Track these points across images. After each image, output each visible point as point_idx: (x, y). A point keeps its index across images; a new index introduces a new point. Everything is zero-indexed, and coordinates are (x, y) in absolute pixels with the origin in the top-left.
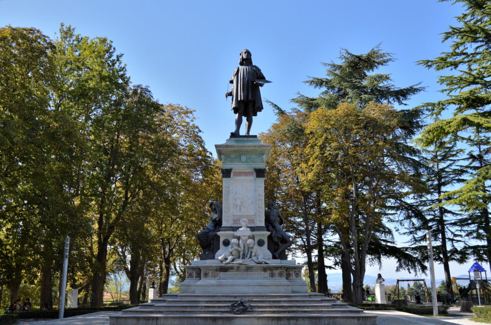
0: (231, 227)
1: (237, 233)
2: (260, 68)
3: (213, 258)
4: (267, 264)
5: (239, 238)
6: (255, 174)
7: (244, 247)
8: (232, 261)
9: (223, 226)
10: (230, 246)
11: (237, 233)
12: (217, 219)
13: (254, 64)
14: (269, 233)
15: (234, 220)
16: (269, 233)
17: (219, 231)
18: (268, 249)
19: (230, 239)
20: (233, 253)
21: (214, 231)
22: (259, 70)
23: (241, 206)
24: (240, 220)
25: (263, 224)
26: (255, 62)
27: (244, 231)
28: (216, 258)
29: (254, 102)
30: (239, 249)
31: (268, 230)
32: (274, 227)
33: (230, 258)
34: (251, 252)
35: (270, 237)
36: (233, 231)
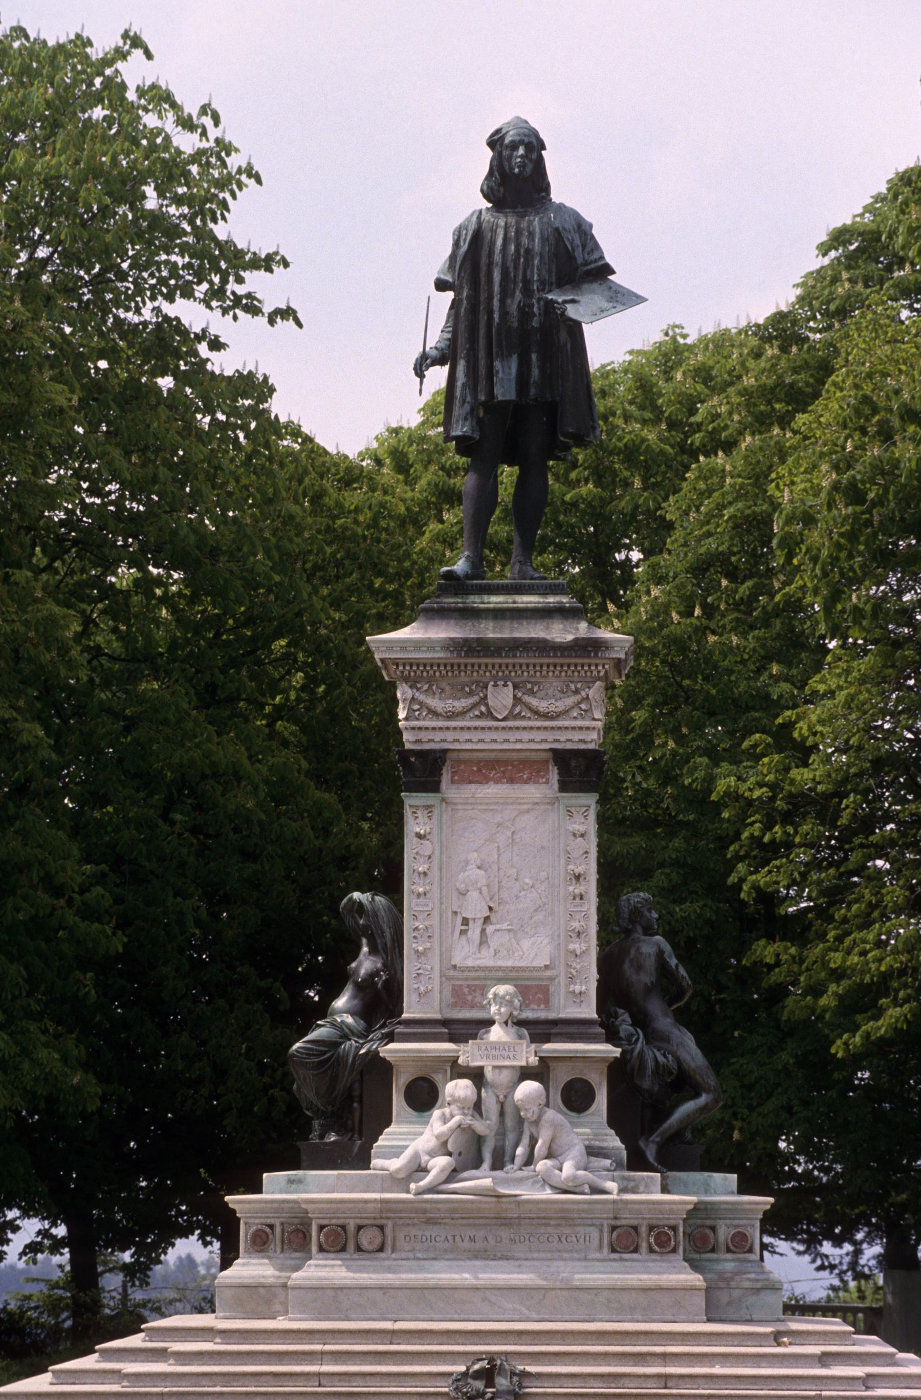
0: (445, 1023)
1: (468, 1054)
2: (587, 215)
3: (364, 1162)
4: (603, 1192)
5: (477, 1076)
6: (554, 775)
7: (502, 1114)
8: (450, 1179)
9: (405, 1016)
10: (436, 1113)
11: (468, 1054)
12: (379, 982)
13: (557, 195)
14: (613, 1051)
15: (457, 992)
16: (613, 1051)
17: (390, 1038)
18: (613, 1122)
19: (438, 1078)
20: (450, 1147)
21: (364, 1035)
22: (583, 229)
23: (487, 920)
24: (484, 990)
25: (589, 1011)
26: (566, 187)
27: (501, 1046)
28: (375, 1162)
29: (552, 410)
30: (480, 1127)
31: (612, 1037)
32: (641, 1020)
33: (440, 1164)
34: (533, 1141)
35: (617, 1071)
36: (453, 1038)
